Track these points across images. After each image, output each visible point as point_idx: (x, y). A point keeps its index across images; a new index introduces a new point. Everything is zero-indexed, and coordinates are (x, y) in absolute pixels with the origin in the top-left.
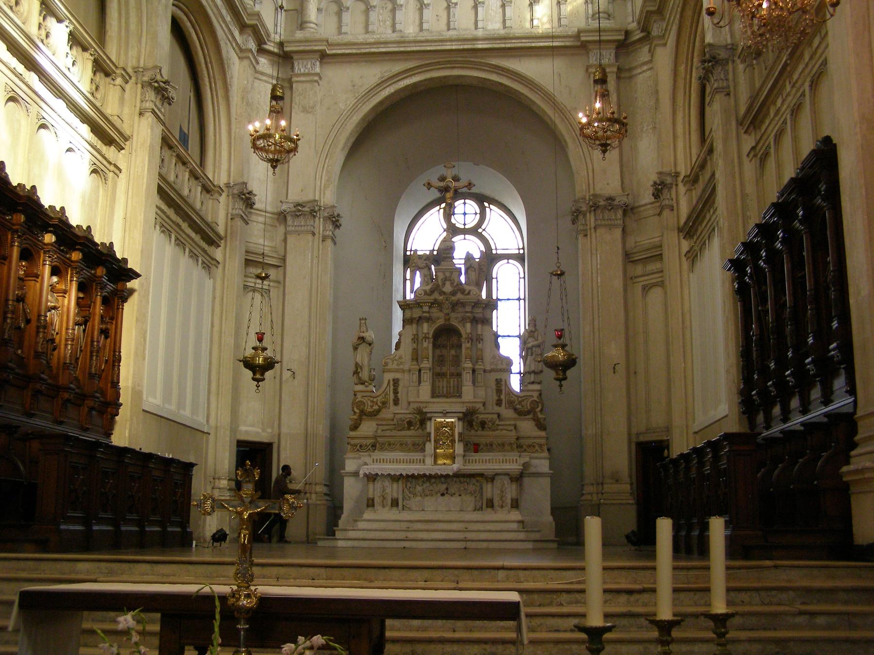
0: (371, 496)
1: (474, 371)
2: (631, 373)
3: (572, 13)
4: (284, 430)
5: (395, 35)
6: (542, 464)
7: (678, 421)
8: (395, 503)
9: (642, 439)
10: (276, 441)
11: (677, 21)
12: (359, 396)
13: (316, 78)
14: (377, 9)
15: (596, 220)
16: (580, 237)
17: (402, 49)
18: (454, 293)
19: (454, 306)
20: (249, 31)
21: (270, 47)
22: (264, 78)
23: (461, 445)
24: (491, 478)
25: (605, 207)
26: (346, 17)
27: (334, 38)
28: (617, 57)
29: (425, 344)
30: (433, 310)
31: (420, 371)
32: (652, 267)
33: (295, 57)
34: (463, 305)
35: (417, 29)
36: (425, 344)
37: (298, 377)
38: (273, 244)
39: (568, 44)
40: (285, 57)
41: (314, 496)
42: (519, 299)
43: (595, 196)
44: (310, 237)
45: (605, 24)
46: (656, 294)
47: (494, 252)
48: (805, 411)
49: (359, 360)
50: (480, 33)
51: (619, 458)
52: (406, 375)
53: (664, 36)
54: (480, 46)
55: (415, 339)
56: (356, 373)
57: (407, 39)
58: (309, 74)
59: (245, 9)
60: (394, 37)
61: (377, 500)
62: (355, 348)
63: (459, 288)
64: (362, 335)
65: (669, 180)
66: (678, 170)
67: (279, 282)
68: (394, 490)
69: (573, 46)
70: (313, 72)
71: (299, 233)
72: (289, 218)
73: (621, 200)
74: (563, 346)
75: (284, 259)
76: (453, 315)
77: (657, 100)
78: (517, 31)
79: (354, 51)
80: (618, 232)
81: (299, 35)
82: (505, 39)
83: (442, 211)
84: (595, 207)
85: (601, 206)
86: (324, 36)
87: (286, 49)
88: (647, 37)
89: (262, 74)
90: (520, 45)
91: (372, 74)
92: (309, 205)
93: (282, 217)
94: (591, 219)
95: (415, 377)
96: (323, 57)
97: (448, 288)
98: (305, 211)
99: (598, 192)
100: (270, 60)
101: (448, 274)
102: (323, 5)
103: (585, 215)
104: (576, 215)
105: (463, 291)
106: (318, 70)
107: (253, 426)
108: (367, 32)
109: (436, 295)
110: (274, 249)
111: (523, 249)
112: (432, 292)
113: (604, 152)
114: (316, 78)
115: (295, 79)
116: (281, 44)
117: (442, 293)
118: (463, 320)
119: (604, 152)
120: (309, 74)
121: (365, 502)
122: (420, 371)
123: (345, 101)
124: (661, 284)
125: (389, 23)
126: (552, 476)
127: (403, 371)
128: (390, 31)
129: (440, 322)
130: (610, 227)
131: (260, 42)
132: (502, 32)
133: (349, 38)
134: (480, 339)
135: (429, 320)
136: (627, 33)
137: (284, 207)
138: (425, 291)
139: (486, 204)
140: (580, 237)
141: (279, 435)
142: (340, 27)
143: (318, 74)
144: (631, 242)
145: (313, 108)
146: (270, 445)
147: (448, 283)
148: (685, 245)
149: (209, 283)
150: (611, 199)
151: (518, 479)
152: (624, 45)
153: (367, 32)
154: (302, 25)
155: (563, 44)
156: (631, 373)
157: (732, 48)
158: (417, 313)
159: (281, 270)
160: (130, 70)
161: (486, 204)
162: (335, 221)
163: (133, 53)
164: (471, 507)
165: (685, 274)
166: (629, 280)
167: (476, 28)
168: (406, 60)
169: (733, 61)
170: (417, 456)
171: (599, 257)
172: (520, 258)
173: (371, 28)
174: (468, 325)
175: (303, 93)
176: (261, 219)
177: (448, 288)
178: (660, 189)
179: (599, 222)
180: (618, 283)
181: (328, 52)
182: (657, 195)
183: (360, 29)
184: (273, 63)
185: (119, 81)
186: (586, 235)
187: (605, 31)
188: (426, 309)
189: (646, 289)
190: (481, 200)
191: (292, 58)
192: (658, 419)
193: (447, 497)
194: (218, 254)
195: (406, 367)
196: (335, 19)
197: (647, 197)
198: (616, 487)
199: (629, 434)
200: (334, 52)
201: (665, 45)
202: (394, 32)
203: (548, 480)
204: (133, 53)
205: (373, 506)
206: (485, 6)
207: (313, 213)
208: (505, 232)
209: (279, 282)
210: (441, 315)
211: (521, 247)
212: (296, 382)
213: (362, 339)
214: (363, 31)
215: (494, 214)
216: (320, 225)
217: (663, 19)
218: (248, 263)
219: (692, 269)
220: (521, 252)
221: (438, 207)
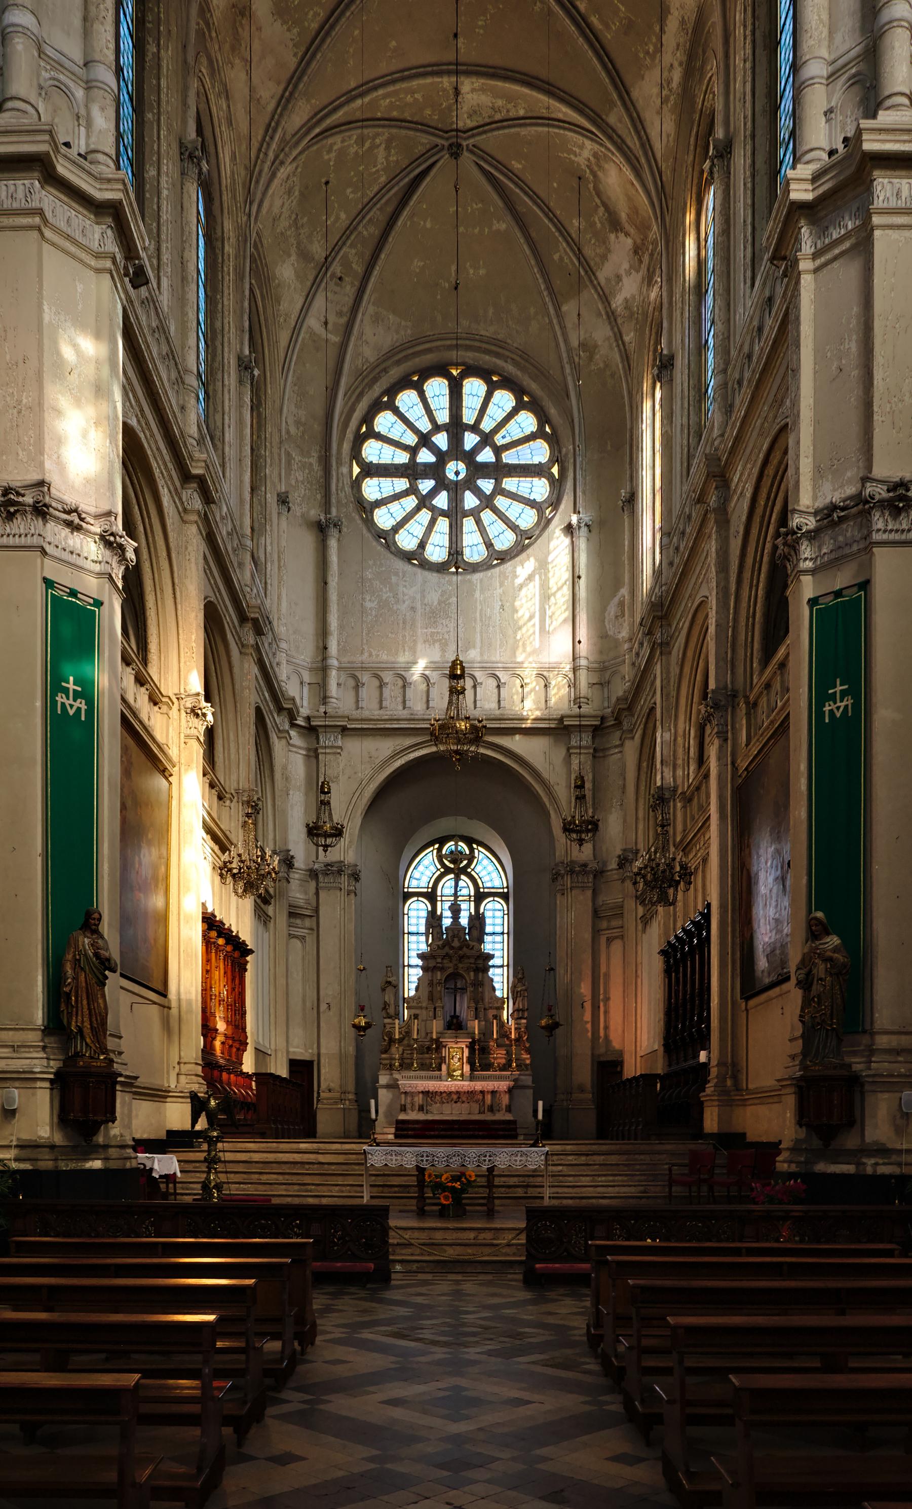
0: (403, 1103)
1: (476, 1009)
3: (556, 703)
4: (323, 1051)
5: (405, 712)
7: (628, 1049)
9: (602, 1059)
10: (315, 1058)
11: (642, 726)
12: (388, 1026)
13: (339, 751)
14: (389, 686)
15: (572, 882)
16: (559, 896)
17: (412, 726)
18: (460, 948)
19: (461, 958)
20: (285, 713)
21: (300, 722)
22: (294, 749)
23: (468, 1067)
25: (580, 872)
26: (363, 692)
27: (356, 714)
28: (593, 738)
29: (439, 988)
30: (445, 961)
31: (435, 1009)
32: (615, 923)
33: (320, 730)
34: (469, 957)
35: (425, 706)
36: (439, 988)
37: (333, 1009)
38: (307, 897)
39: (553, 726)
40: (311, 730)
41: (347, 1102)
42: (503, 933)
43: (572, 861)
44: (338, 892)
45: (585, 709)
46: (617, 946)
47: (482, 890)
48: (686, 1061)
49: (387, 999)
52: (424, 1012)
53: (632, 731)
55: (431, 984)
56: (384, 1008)
57: (416, 717)
58: (332, 747)
59: (283, 695)
60: (405, 714)
61: (408, 1106)
62: (383, 990)
64: (389, 979)
65: (631, 856)
66: (639, 847)
67: (312, 929)
69: (558, 729)
70: (336, 745)
71: (329, 889)
72: (320, 876)
73: (593, 866)
74: (551, 1016)
75: (317, 910)
76: (460, 965)
77: (625, 779)
78: (508, 713)
79: (371, 726)
80: (589, 893)
82: (500, 720)
83: (435, 851)
84: (572, 872)
85: (577, 870)
86: (346, 713)
87: (313, 723)
88: (618, 723)
89: (293, 746)
90: (512, 726)
91: (385, 747)
92: (337, 865)
93: (313, 874)
94: (568, 881)
95: (431, 1014)
96: (344, 729)
97: (456, 944)
98: (334, 870)
99: (574, 858)
100: (299, 732)
101: (456, 932)
102: (342, 680)
103: (563, 878)
104: (556, 877)
105: (468, 946)
106: (340, 743)
107: (298, 1047)
108: (381, 708)
109: (447, 949)
110: (308, 902)
111: (507, 887)
112: (444, 946)
113: (580, 845)
114: (339, 751)
115: (320, 751)
116: (308, 719)
117: (452, 948)
118: (468, 970)
119: (580, 845)
120: (332, 747)
121: (399, 1107)
122: (435, 1009)
124: (622, 937)
125: (400, 699)
126: (533, 1088)
127: (421, 1008)
128: (401, 707)
129: (450, 971)
130: (583, 888)
131: (292, 716)
132: (498, 712)
133: (366, 714)
134: (481, 984)
135: (442, 969)
137: (316, 866)
138: (438, 946)
139: (475, 846)
140: (559, 896)
141: (319, 1055)
142: (357, 701)
143: (341, 748)
144: (601, 899)
145: (337, 777)
146: (312, 1062)
147: (456, 939)
148: (641, 911)
149: (266, 935)
150: (585, 865)
152: (598, 730)
153: (381, 708)
154: (325, 699)
155: (547, 726)
158: (432, 964)
159: (314, 919)
160: (233, 792)
161: (475, 846)
163: (234, 777)
164: (477, 1112)
165: (639, 933)
166: (596, 932)
167: (475, 708)
168: (415, 735)
169: (674, 800)
171: (572, 913)
172: (505, 897)
173: (384, 704)
174: (472, 974)
176: (297, 876)
177: (456, 944)
178: (623, 862)
179: (574, 885)
180: (588, 936)
181: (349, 726)
182: (621, 866)
183: (375, 705)
185: (228, 802)
186: (563, 894)
187: (584, 717)
188: (439, 960)
189: (609, 940)
191: (317, 731)
193: (459, 1104)
194: (270, 910)
195: (424, 1005)
196: (352, 693)
197: (613, 865)
199: (593, 1054)
200: (353, 726)
201: (633, 738)
202: (404, 708)
203: (531, 1091)
204: (234, 777)
205: (405, 1110)
206: (483, 686)
207: (340, 872)
208: (490, 871)
209: (312, 929)
210: (451, 965)
211: (505, 885)
212: (331, 1013)
213: (389, 983)
214: (377, 706)
215: (481, 854)
216: (344, 880)
217: (633, 716)
218: (291, 915)
219: (644, 931)
220: (506, 890)
221: (431, 848)
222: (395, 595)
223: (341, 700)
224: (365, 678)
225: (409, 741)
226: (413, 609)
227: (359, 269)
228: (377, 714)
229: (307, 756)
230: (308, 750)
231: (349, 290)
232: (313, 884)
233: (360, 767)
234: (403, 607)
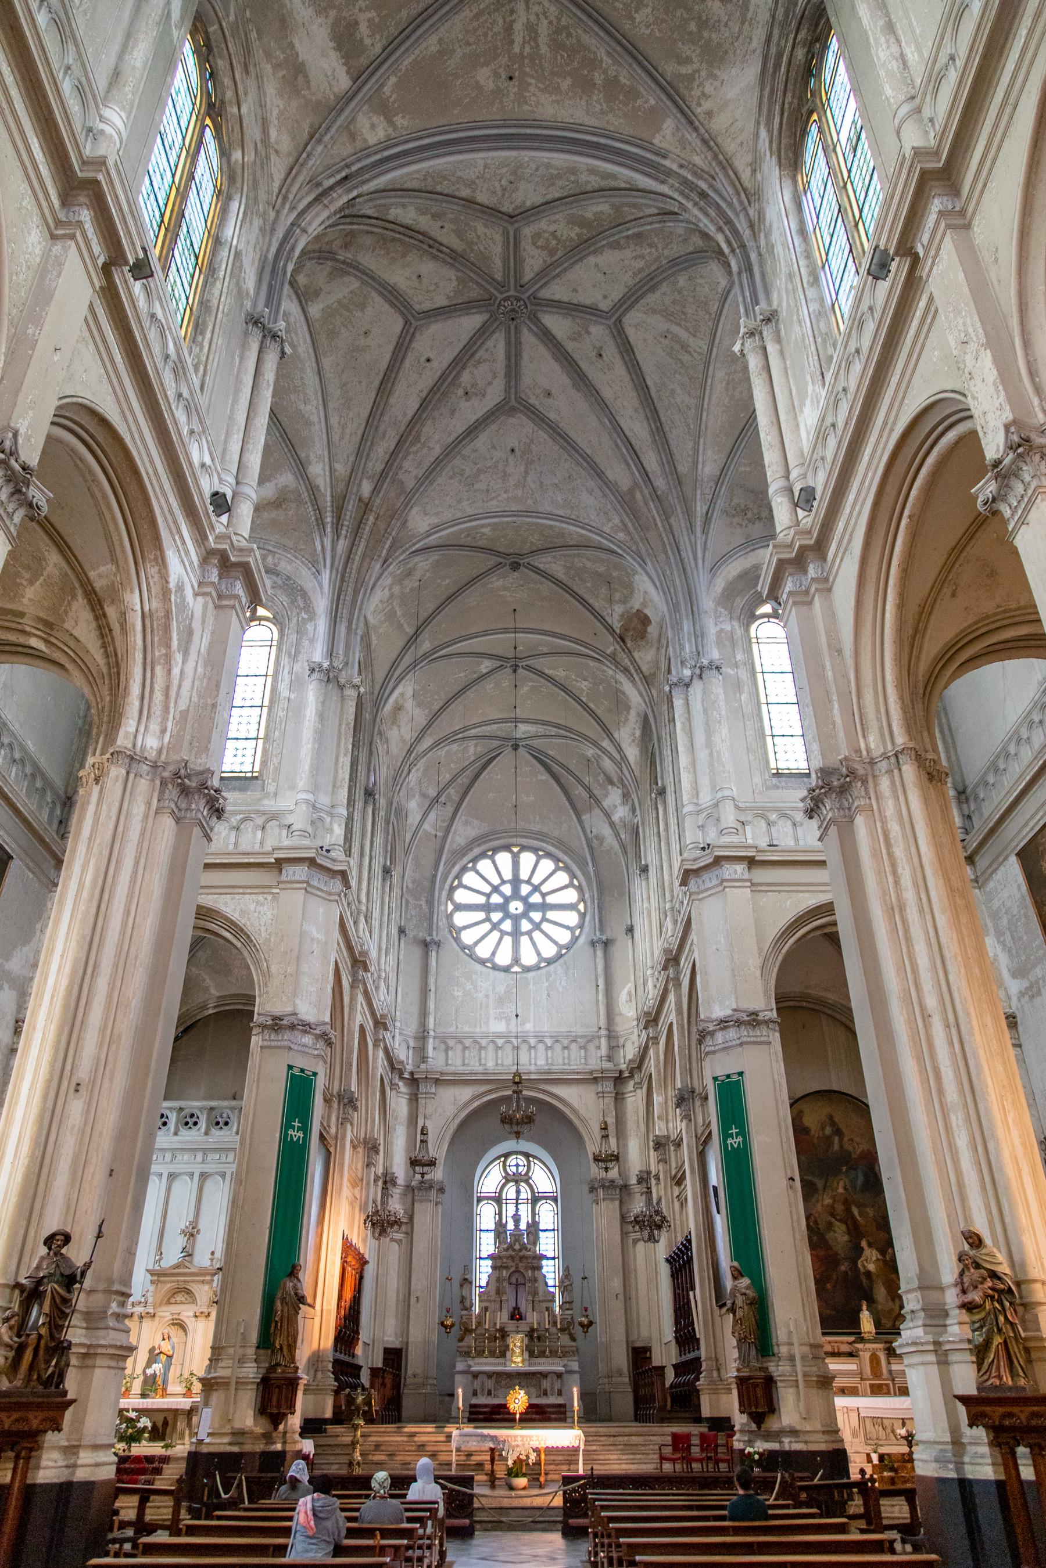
2: (627, 1298)
6: (575, 1366)
7: (655, 1336)
8: (489, 1393)
24: (544, 1375)
40: (413, 1082)
50: (533, 1068)
51: (621, 1360)
54: (533, 1077)
60: (480, 1069)
63: (523, 1247)
68: (490, 1384)
80: (617, 1203)
81: (423, 1066)
84: (603, 1186)
91: (465, 1094)
94: (601, 1192)
104: (592, 1189)
116: (412, 1073)
123: (450, 1110)
130: (612, 1200)
133: (451, 1069)
136: (621, 1072)
146: (400, 1350)
150: (613, 1181)
151: (559, 1375)
152: (619, 1080)
154: (424, 1059)
156: (627, 1298)
157: (668, 1137)
162: (441, 1190)
170: (501, 1360)
175: (427, 1106)
180: (618, 1238)
183: (459, 1062)
184: (406, 1084)
190: (527, 1155)
192: (644, 1333)
197: (633, 1180)
198: (620, 1380)
222: (475, 987)
223: (436, 1059)
224: (451, 1043)
225: (483, 1089)
226: (487, 996)
227: (457, 799)
228: (461, 1069)
229: (410, 1100)
230: (411, 1094)
231: (450, 809)
232: (410, 1197)
233: (446, 1107)
234: (481, 995)
